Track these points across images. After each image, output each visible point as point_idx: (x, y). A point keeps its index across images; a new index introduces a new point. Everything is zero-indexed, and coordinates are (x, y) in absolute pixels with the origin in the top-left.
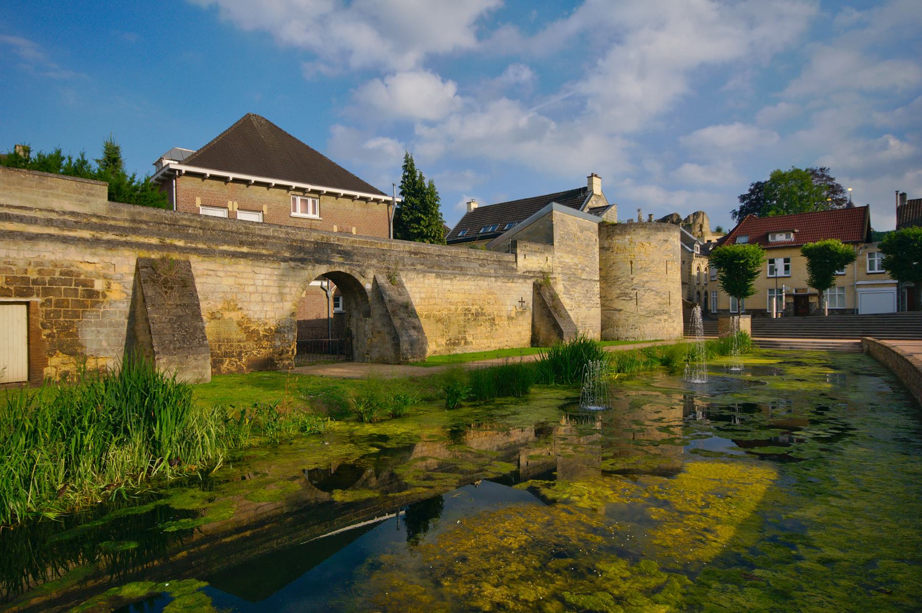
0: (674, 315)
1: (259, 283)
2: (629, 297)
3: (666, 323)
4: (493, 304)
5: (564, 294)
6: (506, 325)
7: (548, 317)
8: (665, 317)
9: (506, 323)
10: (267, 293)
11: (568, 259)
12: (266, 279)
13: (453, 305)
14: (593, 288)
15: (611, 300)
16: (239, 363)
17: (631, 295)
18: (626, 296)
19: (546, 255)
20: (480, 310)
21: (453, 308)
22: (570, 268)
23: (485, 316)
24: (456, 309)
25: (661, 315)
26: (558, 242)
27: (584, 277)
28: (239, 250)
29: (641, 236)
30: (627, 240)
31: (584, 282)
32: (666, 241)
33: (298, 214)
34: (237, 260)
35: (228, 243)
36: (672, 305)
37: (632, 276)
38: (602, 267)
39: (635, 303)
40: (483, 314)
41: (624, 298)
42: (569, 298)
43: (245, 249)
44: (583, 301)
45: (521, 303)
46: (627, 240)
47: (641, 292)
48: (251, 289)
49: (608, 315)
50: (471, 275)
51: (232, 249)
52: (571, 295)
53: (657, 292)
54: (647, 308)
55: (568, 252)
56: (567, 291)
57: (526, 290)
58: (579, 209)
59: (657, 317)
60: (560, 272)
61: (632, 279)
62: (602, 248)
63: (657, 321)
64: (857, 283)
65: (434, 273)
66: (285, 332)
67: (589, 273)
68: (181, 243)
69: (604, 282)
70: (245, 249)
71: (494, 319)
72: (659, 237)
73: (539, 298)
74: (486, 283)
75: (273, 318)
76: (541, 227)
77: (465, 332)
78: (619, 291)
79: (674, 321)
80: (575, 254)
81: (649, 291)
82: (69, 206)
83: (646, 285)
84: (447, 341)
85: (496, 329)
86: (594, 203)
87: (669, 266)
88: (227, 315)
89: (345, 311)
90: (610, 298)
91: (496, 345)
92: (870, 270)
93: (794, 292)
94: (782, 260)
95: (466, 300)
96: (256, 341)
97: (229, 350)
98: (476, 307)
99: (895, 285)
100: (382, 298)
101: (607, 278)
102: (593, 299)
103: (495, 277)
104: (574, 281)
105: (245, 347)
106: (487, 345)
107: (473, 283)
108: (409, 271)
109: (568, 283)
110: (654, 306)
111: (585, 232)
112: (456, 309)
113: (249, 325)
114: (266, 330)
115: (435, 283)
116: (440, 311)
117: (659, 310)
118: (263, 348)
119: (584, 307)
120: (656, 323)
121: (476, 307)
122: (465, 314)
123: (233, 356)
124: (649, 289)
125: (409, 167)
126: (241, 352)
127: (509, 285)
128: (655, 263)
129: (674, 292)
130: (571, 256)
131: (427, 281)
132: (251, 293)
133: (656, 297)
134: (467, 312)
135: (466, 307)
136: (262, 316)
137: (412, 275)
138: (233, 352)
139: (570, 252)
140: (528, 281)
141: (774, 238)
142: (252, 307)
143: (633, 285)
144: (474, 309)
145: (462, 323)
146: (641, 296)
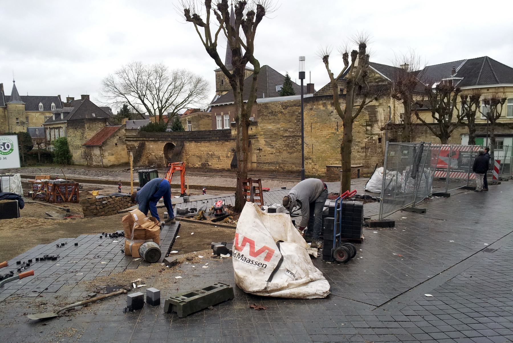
3: (311, 165)
8: (310, 161)
11: (270, 127)
19: (251, 127)
20: (213, 154)
22: (272, 131)
24: (204, 153)
27: (286, 135)
32: (311, 109)
35: (151, 138)
36: (314, 153)
40: (214, 155)
42: (270, 147)
44: (285, 148)
53: (307, 144)
55: (270, 123)
56: (268, 144)
60: (262, 134)
67: (293, 132)
70: (153, 139)
71: (219, 157)
74: (214, 143)
77: (208, 161)
80: (278, 123)
82: (135, 134)
87: (313, 126)
91: (222, 167)
98: (212, 152)
102: (297, 147)
104: (275, 138)
107: (209, 143)
109: (269, 139)
112: (204, 153)
117: (308, 156)
121: (212, 152)
122: (207, 155)
127: (226, 143)
131: (192, 144)
137: (188, 142)
139: (273, 122)
144: (210, 153)
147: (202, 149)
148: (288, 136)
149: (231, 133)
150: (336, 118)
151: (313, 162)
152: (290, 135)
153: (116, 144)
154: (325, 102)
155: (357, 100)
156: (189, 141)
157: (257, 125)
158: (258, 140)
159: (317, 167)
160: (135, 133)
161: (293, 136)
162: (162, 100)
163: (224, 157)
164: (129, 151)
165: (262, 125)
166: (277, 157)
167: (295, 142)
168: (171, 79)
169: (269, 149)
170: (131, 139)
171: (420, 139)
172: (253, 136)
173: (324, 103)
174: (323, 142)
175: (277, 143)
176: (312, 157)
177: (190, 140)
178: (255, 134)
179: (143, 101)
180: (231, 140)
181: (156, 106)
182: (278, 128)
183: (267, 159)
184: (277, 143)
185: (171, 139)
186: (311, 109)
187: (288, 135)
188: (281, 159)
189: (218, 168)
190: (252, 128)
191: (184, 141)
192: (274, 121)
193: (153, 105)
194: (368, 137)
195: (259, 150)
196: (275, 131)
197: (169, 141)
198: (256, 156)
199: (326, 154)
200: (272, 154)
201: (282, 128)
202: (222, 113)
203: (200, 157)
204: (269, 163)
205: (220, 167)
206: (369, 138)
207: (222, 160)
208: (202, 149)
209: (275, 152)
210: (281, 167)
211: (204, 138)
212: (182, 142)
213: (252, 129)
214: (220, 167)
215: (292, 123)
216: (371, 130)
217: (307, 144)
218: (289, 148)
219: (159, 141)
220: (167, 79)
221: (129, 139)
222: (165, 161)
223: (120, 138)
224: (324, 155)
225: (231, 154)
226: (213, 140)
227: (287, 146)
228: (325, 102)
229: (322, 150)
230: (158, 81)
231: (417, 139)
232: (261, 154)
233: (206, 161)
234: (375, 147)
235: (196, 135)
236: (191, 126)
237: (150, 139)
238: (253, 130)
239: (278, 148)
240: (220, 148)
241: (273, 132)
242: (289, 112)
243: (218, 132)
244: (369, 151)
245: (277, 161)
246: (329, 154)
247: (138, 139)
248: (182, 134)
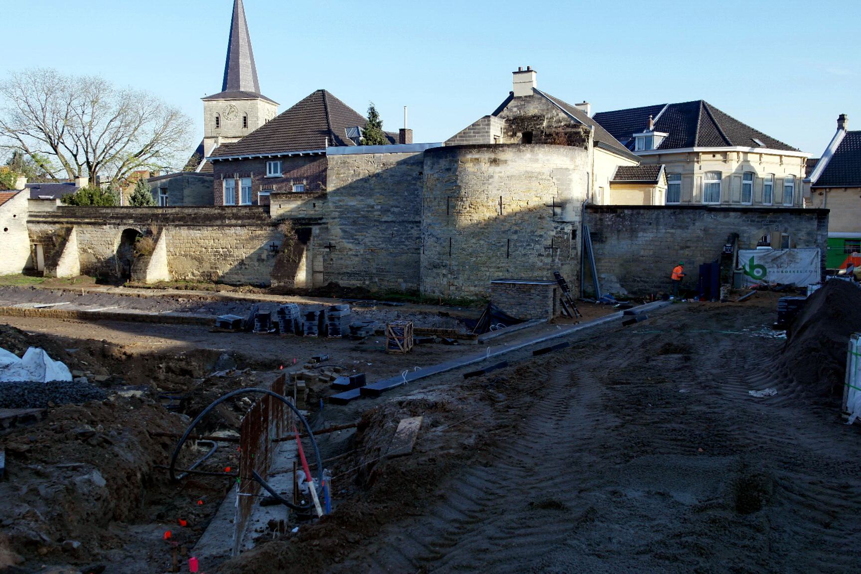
3: (445, 279)
5: (344, 238)
8: (444, 272)
9: (256, 264)
22: (357, 211)
25: (439, 268)
27: (385, 219)
31: (384, 227)
35: (87, 218)
36: (453, 256)
42: (352, 243)
44: (383, 246)
52: (356, 239)
53: (437, 238)
55: (354, 195)
56: (348, 236)
59: (435, 270)
60: (337, 216)
63: (434, 275)
67: (401, 214)
68: (73, 220)
77: (216, 268)
80: (370, 195)
102: (407, 243)
104: (364, 224)
109: (351, 227)
117: (438, 261)
133: (436, 245)
150: (498, 190)
151: (451, 274)
152: (394, 219)
153: (6, 230)
154: (477, 156)
155: (537, 157)
156: (176, 226)
158: (327, 228)
159: (459, 282)
160: (51, 207)
161: (399, 222)
162: (96, 148)
164: (35, 245)
165: (337, 198)
166: (367, 262)
167: (403, 234)
168: (115, 108)
169: (350, 246)
170: (41, 219)
171: (645, 235)
172: (316, 219)
173: (476, 159)
174: (472, 233)
176: (448, 262)
177: (177, 223)
178: (321, 216)
179: (55, 148)
181: (82, 159)
182: (369, 206)
183: (347, 267)
184: (367, 235)
187: (389, 219)
188: (375, 266)
190: (314, 204)
192: (361, 192)
193: (75, 156)
194: (556, 228)
195: (330, 247)
197: (131, 225)
198: (322, 260)
199: (479, 258)
200: (357, 255)
201: (377, 205)
202: (236, 175)
203: (200, 260)
204: (350, 275)
206: (559, 229)
207: (247, 267)
209: (362, 252)
210: (376, 282)
213: (314, 206)
215: (399, 197)
216: (562, 214)
217: (437, 238)
218: (392, 245)
220: (105, 107)
221: (38, 219)
222: (119, 266)
223: (15, 216)
224: (474, 259)
225: (269, 255)
227: (389, 240)
228: (477, 156)
229: (470, 251)
230: (88, 110)
231: (641, 234)
232: (333, 256)
233: (211, 268)
234: (567, 247)
236: (166, 198)
237: (87, 220)
238: (317, 208)
239: (369, 244)
241: (359, 214)
242: (393, 176)
244: (558, 253)
245: (366, 270)
246: (484, 259)
247: (56, 220)
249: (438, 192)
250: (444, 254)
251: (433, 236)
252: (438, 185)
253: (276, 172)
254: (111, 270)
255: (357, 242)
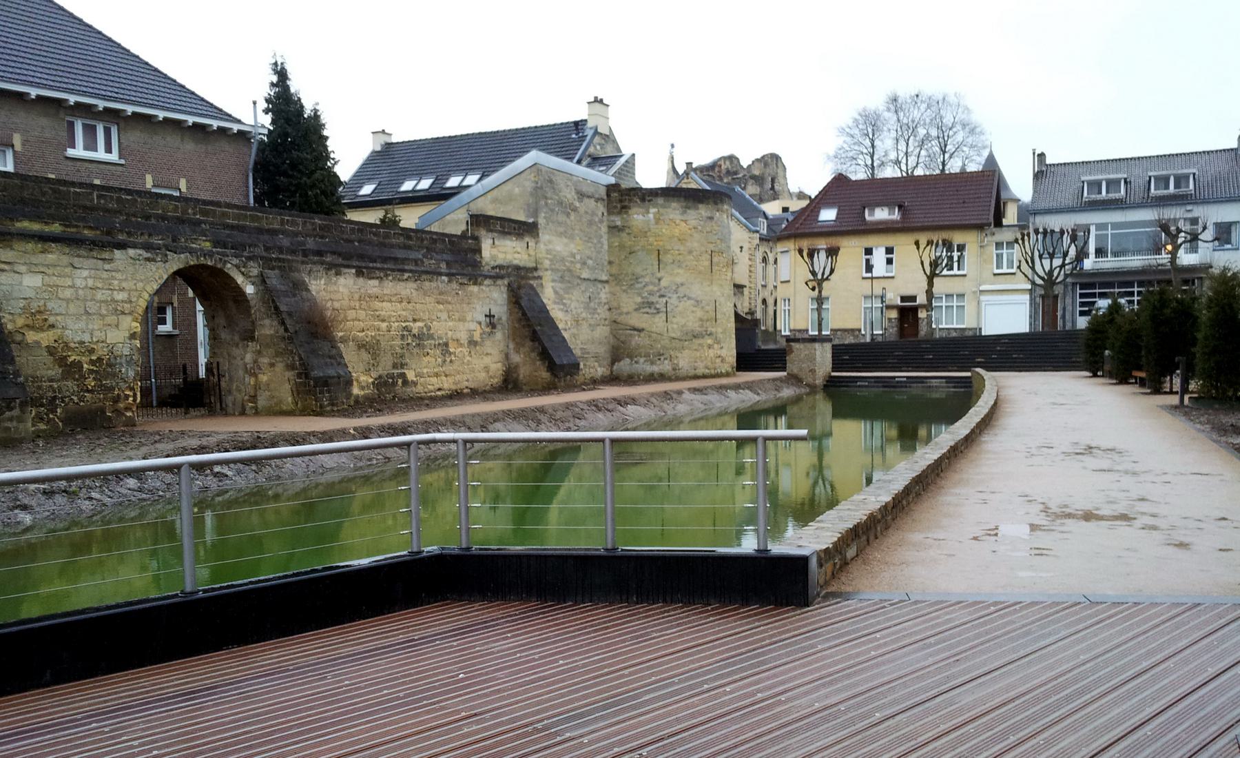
0: (720, 336)
1: (79, 282)
2: (656, 308)
3: (711, 351)
4: (446, 320)
5: (555, 303)
6: (466, 354)
7: (533, 341)
8: (710, 341)
9: (465, 350)
10: (91, 300)
12: (90, 277)
13: (383, 321)
14: (599, 294)
15: (627, 313)
16: (51, 416)
17: (658, 306)
18: (650, 307)
19: (527, 239)
21: (384, 325)
22: (563, 260)
23: (433, 339)
25: (703, 337)
26: (545, 218)
27: (584, 275)
28: (47, 229)
29: (674, 209)
30: (651, 216)
32: (711, 218)
33: (78, 151)
34: (47, 245)
35: (31, 218)
36: (718, 321)
37: (659, 275)
38: (612, 259)
39: (664, 318)
40: (431, 337)
41: (647, 310)
42: (562, 310)
43: (56, 228)
44: (584, 315)
45: (488, 320)
46: (651, 216)
47: (674, 300)
48: (68, 293)
49: (623, 338)
50: (411, 271)
51: (36, 227)
52: (564, 304)
53: (697, 301)
54: (682, 326)
55: (561, 235)
56: (560, 300)
57: (493, 298)
58: (571, 159)
59: (697, 341)
61: (659, 280)
62: (613, 229)
64: (983, 288)
65: (353, 267)
66: (121, 364)
69: (616, 285)
70: (56, 228)
71: (446, 344)
72: (700, 211)
73: (516, 310)
74: (434, 284)
75: (103, 342)
76: (517, 190)
77: (402, 366)
78: (639, 300)
79: (722, 348)
80: (572, 238)
81: (685, 299)
83: (680, 289)
84: (376, 379)
85: (451, 361)
86: (598, 147)
87: (715, 260)
88: (31, 336)
89: (177, 332)
90: (625, 310)
92: (998, 268)
93: (899, 302)
94: (883, 250)
95: (404, 313)
96: (77, 380)
97: (35, 395)
99: (1028, 292)
100: (276, 308)
101: (621, 278)
102: (599, 311)
103: (447, 275)
104: (569, 282)
105: (60, 389)
106: (437, 386)
108: (314, 263)
110: (693, 324)
111: (586, 200)
113: (64, 354)
114: (92, 362)
115: (354, 284)
116: (363, 331)
117: (700, 329)
118: (88, 391)
119: (585, 325)
120: (696, 350)
122: (403, 336)
123: (42, 405)
124: (685, 296)
125: (282, 75)
126: (55, 398)
128: (694, 253)
129: (722, 300)
130: (565, 240)
131: (342, 280)
132: (68, 301)
133: (695, 309)
134: (405, 333)
135: (404, 325)
136: (86, 338)
138: (42, 398)
140: (499, 282)
141: (872, 214)
142: (70, 323)
143: (660, 290)
144: (416, 327)
145: (398, 350)
146: (672, 307)
147: (386, 308)
148: (588, 279)
149: (479, 251)
151: (718, 343)
156: (330, 267)
157: (538, 234)
163: (461, 345)
175: (573, 298)
176: (713, 330)
180: (486, 277)
185: (216, 243)
186: (711, 218)
189: (439, 389)
191: (303, 263)
196: (567, 261)
197: (210, 254)
205: (448, 384)
208: (386, 308)
211: (396, 260)
212: (286, 269)
213: (528, 247)
214: (446, 386)
219: (122, 246)
225: (484, 333)
226: (427, 273)
233: (395, 366)
235: (351, 241)
237: (25, 225)
240: (450, 307)
241: (565, 265)
243: (435, 241)
248: (276, 226)
249: (696, 244)
250: (707, 320)
251: (689, 298)
252: (695, 235)
253: (91, 145)
254: (116, 400)
255: (565, 309)
